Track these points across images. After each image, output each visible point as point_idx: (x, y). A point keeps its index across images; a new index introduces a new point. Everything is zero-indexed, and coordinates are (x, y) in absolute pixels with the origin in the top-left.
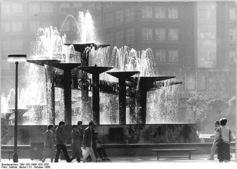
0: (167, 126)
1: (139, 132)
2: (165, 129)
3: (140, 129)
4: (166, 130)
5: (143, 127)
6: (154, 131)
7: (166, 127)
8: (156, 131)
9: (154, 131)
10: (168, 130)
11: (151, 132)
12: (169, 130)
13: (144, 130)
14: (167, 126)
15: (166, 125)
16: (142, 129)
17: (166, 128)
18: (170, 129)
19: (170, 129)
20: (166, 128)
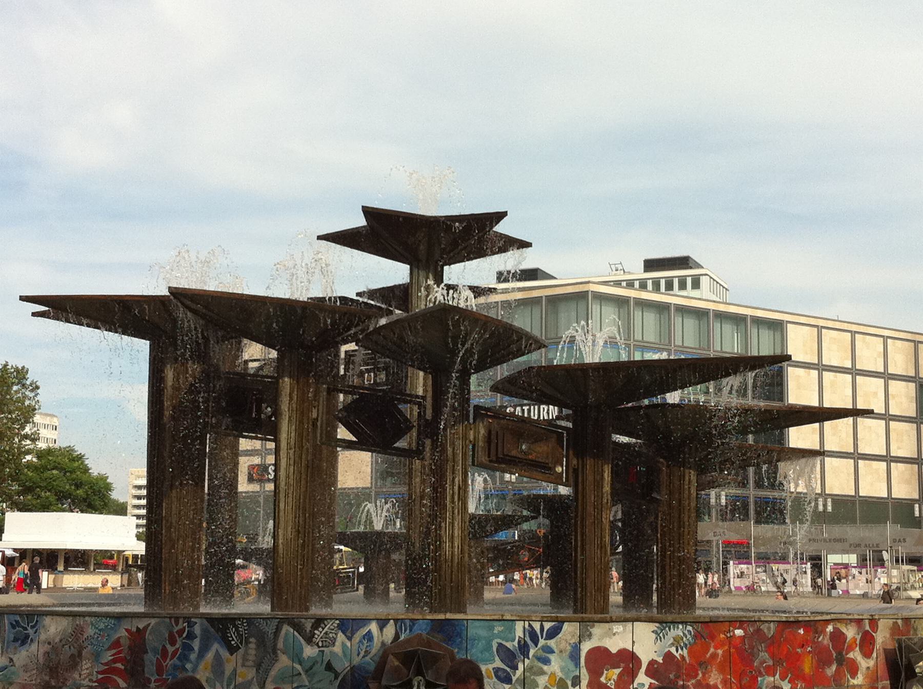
0: (197, 630)
1: (11, 660)
2: (188, 648)
3: (15, 640)
4: (193, 656)
5: (30, 631)
6: (97, 656)
7: (191, 636)
8: (108, 656)
9: (97, 656)
10: (210, 656)
11: (74, 662)
12: (217, 656)
13: (34, 647)
14: (197, 630)
15: (191, 625)
16: (23, 640)
17: (196, 644)
18: (232, 650)
19: (225, 653)
20: (196, 644)
